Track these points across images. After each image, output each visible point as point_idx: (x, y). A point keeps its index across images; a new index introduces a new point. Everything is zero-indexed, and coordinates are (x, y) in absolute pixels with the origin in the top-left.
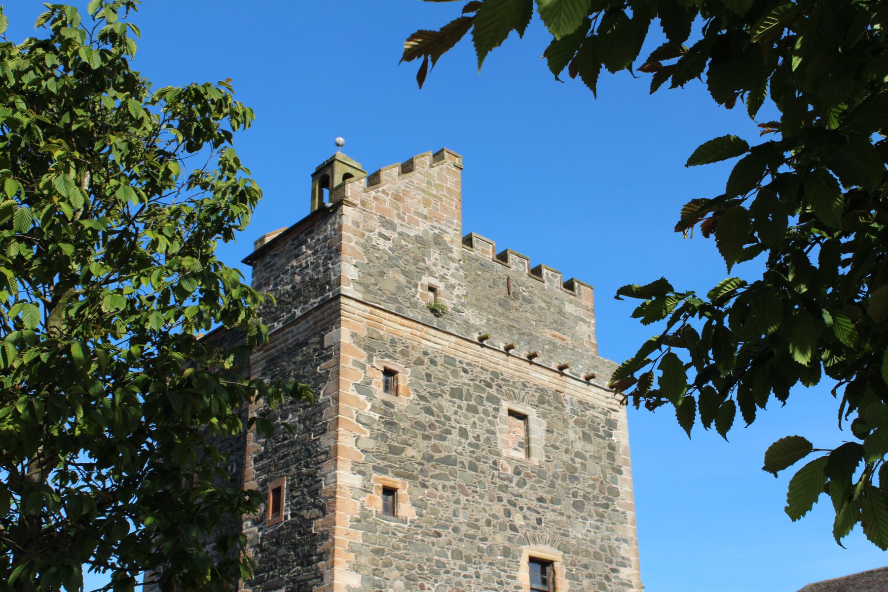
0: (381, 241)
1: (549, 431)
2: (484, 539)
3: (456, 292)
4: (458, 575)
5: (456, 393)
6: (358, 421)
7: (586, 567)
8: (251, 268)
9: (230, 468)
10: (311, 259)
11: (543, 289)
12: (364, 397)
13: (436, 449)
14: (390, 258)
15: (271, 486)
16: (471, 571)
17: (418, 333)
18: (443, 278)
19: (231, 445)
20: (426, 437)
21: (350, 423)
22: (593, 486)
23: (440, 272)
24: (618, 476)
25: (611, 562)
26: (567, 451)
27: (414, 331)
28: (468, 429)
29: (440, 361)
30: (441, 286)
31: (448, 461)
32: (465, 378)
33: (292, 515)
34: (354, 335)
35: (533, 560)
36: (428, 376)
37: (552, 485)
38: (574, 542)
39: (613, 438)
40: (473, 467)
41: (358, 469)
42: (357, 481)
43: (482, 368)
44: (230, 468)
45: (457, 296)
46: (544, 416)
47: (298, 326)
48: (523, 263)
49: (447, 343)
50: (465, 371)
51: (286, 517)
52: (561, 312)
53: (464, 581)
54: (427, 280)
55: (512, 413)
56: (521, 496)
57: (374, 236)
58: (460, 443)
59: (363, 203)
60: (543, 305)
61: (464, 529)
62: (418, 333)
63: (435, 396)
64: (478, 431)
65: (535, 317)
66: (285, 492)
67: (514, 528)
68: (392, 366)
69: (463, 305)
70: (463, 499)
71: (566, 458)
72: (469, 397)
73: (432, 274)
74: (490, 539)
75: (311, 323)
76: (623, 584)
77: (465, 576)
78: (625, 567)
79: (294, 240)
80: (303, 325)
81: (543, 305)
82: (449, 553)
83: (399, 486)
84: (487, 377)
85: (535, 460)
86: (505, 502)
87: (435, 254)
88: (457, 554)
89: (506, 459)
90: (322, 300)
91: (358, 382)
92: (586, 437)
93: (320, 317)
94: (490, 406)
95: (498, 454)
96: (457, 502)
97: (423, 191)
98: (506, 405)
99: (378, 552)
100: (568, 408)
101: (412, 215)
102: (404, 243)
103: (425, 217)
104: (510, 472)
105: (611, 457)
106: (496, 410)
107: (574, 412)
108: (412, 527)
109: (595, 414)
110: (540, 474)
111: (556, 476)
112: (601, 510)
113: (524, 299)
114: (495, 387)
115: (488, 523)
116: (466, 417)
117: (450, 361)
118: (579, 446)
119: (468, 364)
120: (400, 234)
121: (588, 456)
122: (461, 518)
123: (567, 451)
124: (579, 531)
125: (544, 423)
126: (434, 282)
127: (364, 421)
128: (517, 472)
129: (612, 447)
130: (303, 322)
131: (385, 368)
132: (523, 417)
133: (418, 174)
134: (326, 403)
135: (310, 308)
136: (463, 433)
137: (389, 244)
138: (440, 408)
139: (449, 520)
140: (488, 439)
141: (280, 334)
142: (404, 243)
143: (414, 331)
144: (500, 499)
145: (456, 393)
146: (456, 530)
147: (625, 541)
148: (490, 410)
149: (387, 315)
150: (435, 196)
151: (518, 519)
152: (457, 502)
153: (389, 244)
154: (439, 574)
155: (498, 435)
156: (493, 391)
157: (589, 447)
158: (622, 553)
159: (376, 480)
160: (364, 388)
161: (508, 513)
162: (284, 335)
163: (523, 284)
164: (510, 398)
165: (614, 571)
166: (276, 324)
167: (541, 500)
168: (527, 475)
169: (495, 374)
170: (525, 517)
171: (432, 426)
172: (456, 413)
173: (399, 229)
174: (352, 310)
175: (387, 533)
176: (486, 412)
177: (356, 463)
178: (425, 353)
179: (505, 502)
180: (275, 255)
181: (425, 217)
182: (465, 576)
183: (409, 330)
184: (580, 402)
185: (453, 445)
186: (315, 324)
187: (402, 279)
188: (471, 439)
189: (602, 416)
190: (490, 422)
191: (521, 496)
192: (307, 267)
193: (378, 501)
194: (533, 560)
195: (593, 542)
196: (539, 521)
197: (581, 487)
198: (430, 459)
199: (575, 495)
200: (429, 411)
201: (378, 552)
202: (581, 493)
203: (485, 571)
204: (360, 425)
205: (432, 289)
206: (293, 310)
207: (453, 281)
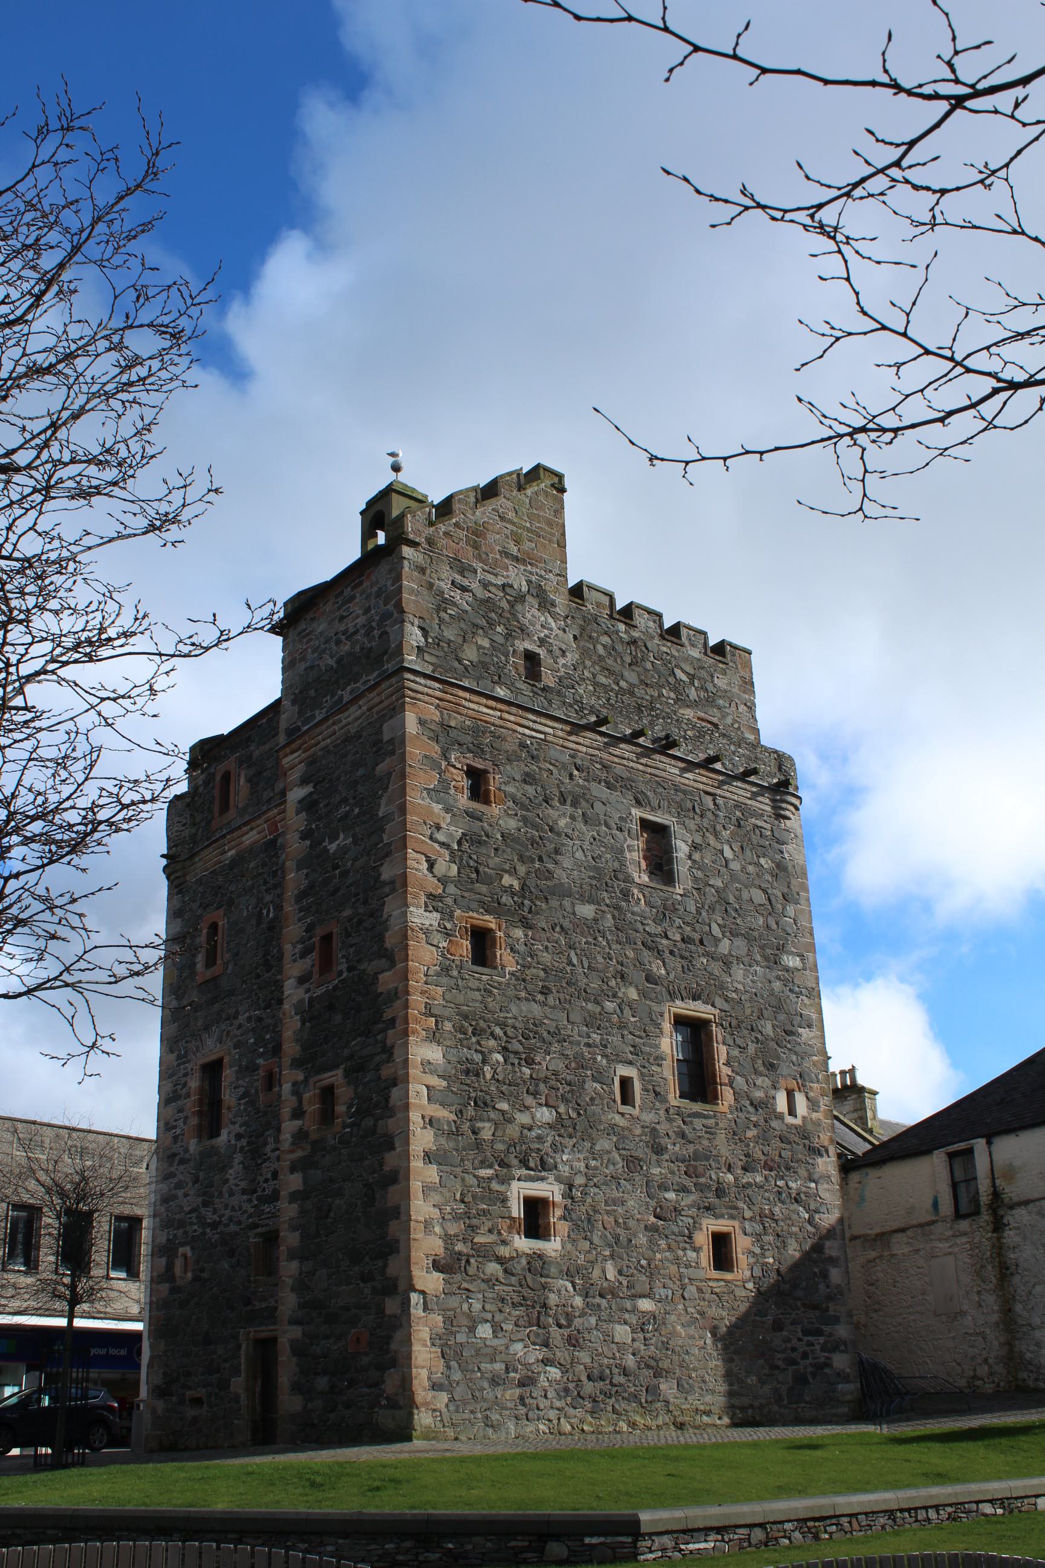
0: (457, 595)
4: (578, 1043)
6: (431, 838)
8: (281, 639)
9: (265, 912)
10: (361, 621)
12: (440, 806)
15: (320, 931)
17: (512, 718)
18: (542, 642)
19: (265, 882)
21: (423, 842)
27: (506, 716)
30: (542, 652)
33: (350, 969)
34: (422, 722)
35: (680, 1022)
38: (734, 995)
41: (434, 901)
42: (432, 919)
43: (601, 763)
44: (265, 912)
45: (564, 665)
47: (347, 713)
49: (551, 731)
51: (340, 973)
57: (445, 586)
59: (430, 542)
60: (684, 678)
62: (512, 718)
65: (672, 695)
66: (336, 943)
68: (479, 764)
74: (620, 995)
75: (365, 708)
77: (588, 1045)
79: (336, 597)
80: (354, 712)
81: (684, 678)
83: (493, 926)
87: (530, 613)
90: (379, 675)
91: (432, 786)
93: (377, 700)
97: (514, 524)
99: (466, 1017)
101: (498, 556)
102: (488, 595)
103: (517, 559)
108: (513, 982)
109: (759, 823)
127: (440, 837)
130: (353, 709)
131: (468, 765)
133: (504, 500)
134: (388, 818)
135: (363, 688)
141: (324, 727)
142: (488, 595)
143: (506, 716)
149: (467, 695)
150: (529, 530)
155: (628, 855)
159: (460, 918)
160: (439, 792)
162: (328, 728)
166: (317, 712)
174: (420, 688)
175: (479, 990)
177: (430, 896)
178: (523, 745)
180: (313, 619)
181: (517, 559)
182: (588, 1045)
183: (499, 714)
186: (369, 709)
192: (357, 632)
193: (465, 946)
194: (680, 1022)
201: (466, 1017)
204: (436, 845)
206: (340, 692)
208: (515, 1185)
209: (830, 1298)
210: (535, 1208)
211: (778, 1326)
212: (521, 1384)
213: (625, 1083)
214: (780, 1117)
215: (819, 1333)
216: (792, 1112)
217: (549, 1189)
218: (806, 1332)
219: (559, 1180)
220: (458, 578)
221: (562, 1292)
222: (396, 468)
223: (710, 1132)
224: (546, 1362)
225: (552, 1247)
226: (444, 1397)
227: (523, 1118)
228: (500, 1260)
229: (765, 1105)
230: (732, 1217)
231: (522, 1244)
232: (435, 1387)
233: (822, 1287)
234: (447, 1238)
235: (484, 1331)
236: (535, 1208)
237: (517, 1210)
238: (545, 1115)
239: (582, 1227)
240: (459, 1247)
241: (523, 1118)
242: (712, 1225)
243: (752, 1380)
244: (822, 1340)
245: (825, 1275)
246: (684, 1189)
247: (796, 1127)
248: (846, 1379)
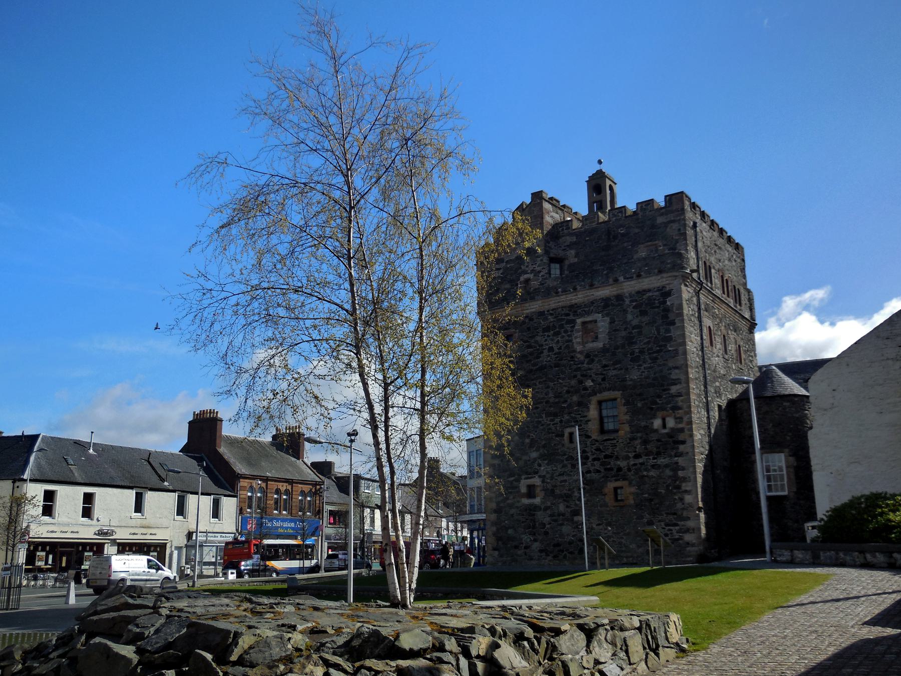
1: (612, 322)
2: (566, 401)
3: (542, 274)
5: (547, 329)
7: (640, 395)
11: (638, 219)
13: (534, 365)
14: (502, 278)
16: (557, 420)
20: (528, 362)
22: (648, 343)
23: (531, 267)
24: (671, 327)
25: (662, 385)
26: (625, 329)
28: (554, 345)
29: (534, 317)
30: (531, 276)
31: (542, 368)
32: (551, 318)
36: (529, 329)
37: (614, 354)
38: (630, 383)
39: (668, 303)
40: (557, 365)
46: (607, 315)
48: (621, 212)
50: (551, 314)
52: (653, 226)
53: (553, 428)
54: (522, 279)
55: (584, 323)
56: (590, 369)
58: (549, 356)
60: (637, 231)
61: (551, 400)
63: (533, 337)
64: (561, 344)
67: (585, 389)
69: (546, 279)
70: (551, 384)
71: (623, 333)
72: (554, 327)
73: (526, 272)
76: (673, 396)
78: (676, 384)
82: (544, 416)
84: (566, 311)
85: (600, 345)
86: (579, 376)
88: (549, 414)
89: (579, 352)
92: (643, 313)
94: (568, 327)
95: (575, 351)
96: (548, 387)
98: (579, 321)
100: (627, 301)
104: (582, 358)
105: (666, 317)
106: (574, 327)
107: (632, 301)
110: (604, 350)
111: (617, 348)
112: (655, 355)
113: (623, 235)
114: (572, 314)
115: (568, 392)
116: (552, 340)
117: (541, 314)
118: (635, 322)
119: (553, 310)
120: (507, 262)
121: (643, 325)
122: (551, 395)
123: (625, 329)
124: (634, 375)
125: (608, 319)
126: (526, 276)
128: (588, 356)
129: (667, 310)
132: (595, 321)
136: (551, 349)
137: (501, 271)
138: (536, 342)
139: (543, 398)
140: (567, 347)
144: (575, 376)
145: (547, 329)
146: (547, 402)
147: (676, 368)
148: (569, 329)
151: (589, 383)
152: (548, 387)
153: (501, 271)
154: (537, 427)
155: (574, 341)
156: (571, 317)
157: (645, 319)
158: (673, 377)
161: (581, 382)
163: (621, 226)
164: (581, 315)
165: (664, 390)
167: (605, 366)
168: (596, 356)
169: (571, 307)
170: (593, 381)
171: (531, 354)
172: (546, 340)
173: (506, 259)
176: (566, 332)
179: (579, 376)
184: (638, 292)
185: (546, 358)
187: (508, 286)
188: (556, 350)
189: (657, 293)
190: (569, 336)
191: (590, 369)
195: (647, 378)
196: (603, 379)
197: (636, 348)
198: (531, 371)
199: (632, 353)
200: (529, 347)
202: (637, 351)
203: (566, 417)
205: (527, 281)
207: (538, 269)
208: (523, 481)
209: (683, 509)
210: (531, 487)
211: (650, 523)
212: (526, 548)
213: (571, 435)
214: (656, 431)
215: (676, 525)
216: (664, 426)
217: (536, 481)
218: (667, 525)
219: (540, 477)
220: (498, 266)
221: (540, 516)
222: (600, 162)
223: (615, 446)
224: (535, 540)
225: (537, 501)
226: (496, 553)
227: (525, 458)
228: (517, 507)
229: (648, 429)
230: (624, 479)
231: (526, 501)
232: (494, 549)
233: (679, 505)
234: (498, 503)
235: (510, 531)
236: (531, 487)
237: (524, 490)
238: (534, 455)
239: (550, 492)
240: (502, 505)
241: (525, 458)
242: (611, 485)
243: (633, 546)
244: (677, 528)
245: (682, 499)
246: (598, 471)
247: (667, 434)
248: (693, 545)
